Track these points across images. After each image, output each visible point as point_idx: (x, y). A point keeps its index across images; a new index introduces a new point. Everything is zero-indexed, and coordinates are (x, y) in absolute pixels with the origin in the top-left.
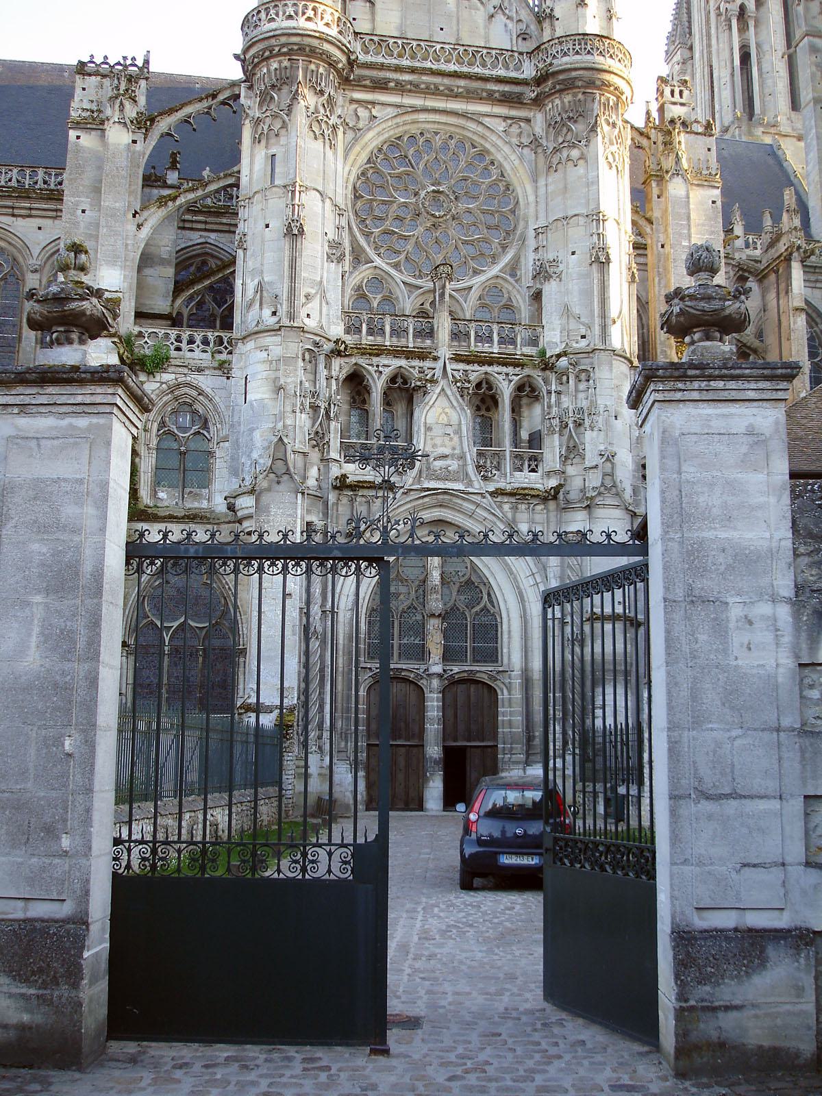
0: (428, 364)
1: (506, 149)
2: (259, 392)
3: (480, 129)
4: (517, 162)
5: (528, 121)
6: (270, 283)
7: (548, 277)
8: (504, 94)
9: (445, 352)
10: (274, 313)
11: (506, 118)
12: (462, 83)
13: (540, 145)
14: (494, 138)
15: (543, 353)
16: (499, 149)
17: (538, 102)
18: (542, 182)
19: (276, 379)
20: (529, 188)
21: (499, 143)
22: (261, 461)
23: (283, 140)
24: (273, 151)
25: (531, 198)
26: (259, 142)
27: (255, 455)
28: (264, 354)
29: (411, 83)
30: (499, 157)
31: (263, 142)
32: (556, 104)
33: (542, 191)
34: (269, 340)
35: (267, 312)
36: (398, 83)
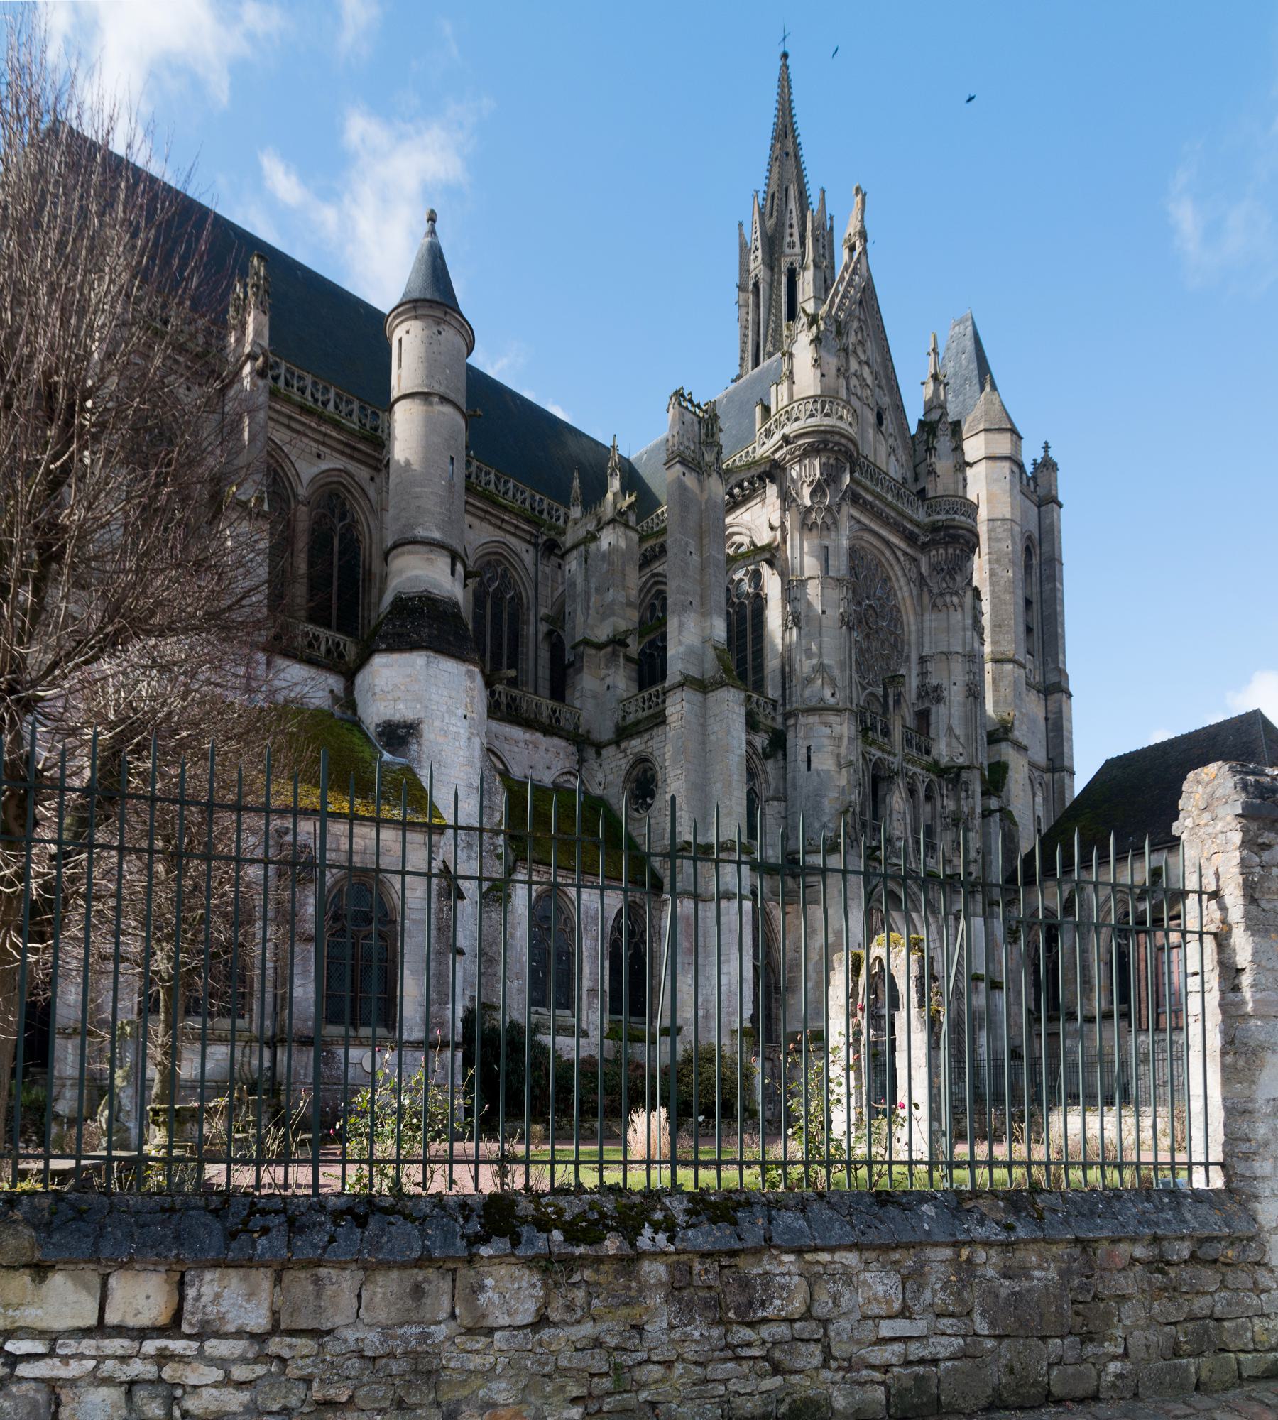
0: (891, 759)
1: (902, 581)
2: (824, 762)
3: (891, 558)
4: (907, 594)
5: (915, 560)
6: (829, 666)
7: (939, 700)
8: (912, 533)
9: (898, 750)
10: (833, 695)
11: (905, 554)
12: (893, 514)
13: (927, 585)
14: (897, 568)
15: (936, 762)
16: (898, 580)
17: (924, 548)
18: (927, 617)
19: (838, 755)
20: (912, 619)
21: (900, 573)
22: (831, 825)
23: (833, 535)
24: (826, 542)
25: (913, 628)
26: (810, 530)
27: (825, 819)
28: (828, 731)
29: (871, 503)
30: (896, 585)
31: (815, 532)
32: (940, 554)
33: (927, 625)
34: (832, 718)
35: (827, 693)
36: (865, 501)
